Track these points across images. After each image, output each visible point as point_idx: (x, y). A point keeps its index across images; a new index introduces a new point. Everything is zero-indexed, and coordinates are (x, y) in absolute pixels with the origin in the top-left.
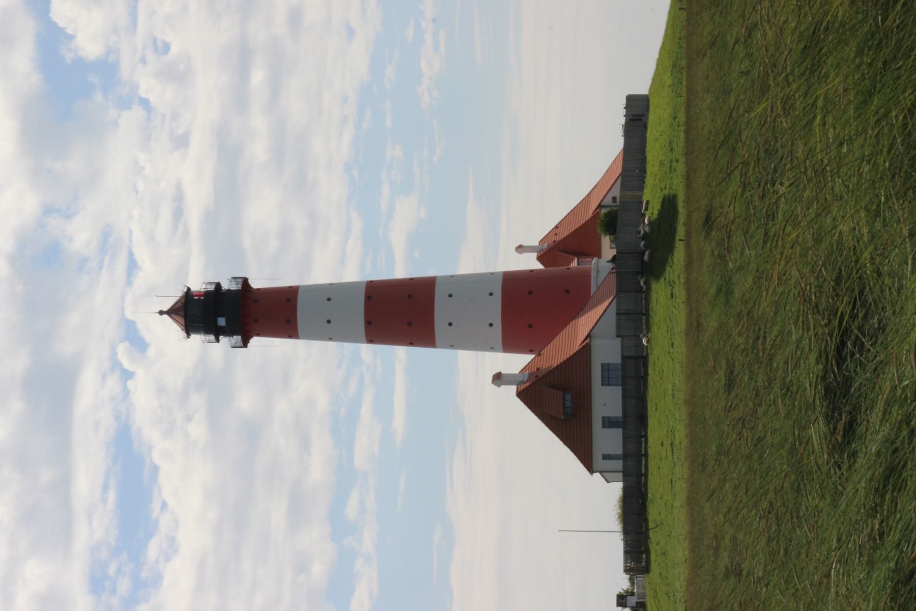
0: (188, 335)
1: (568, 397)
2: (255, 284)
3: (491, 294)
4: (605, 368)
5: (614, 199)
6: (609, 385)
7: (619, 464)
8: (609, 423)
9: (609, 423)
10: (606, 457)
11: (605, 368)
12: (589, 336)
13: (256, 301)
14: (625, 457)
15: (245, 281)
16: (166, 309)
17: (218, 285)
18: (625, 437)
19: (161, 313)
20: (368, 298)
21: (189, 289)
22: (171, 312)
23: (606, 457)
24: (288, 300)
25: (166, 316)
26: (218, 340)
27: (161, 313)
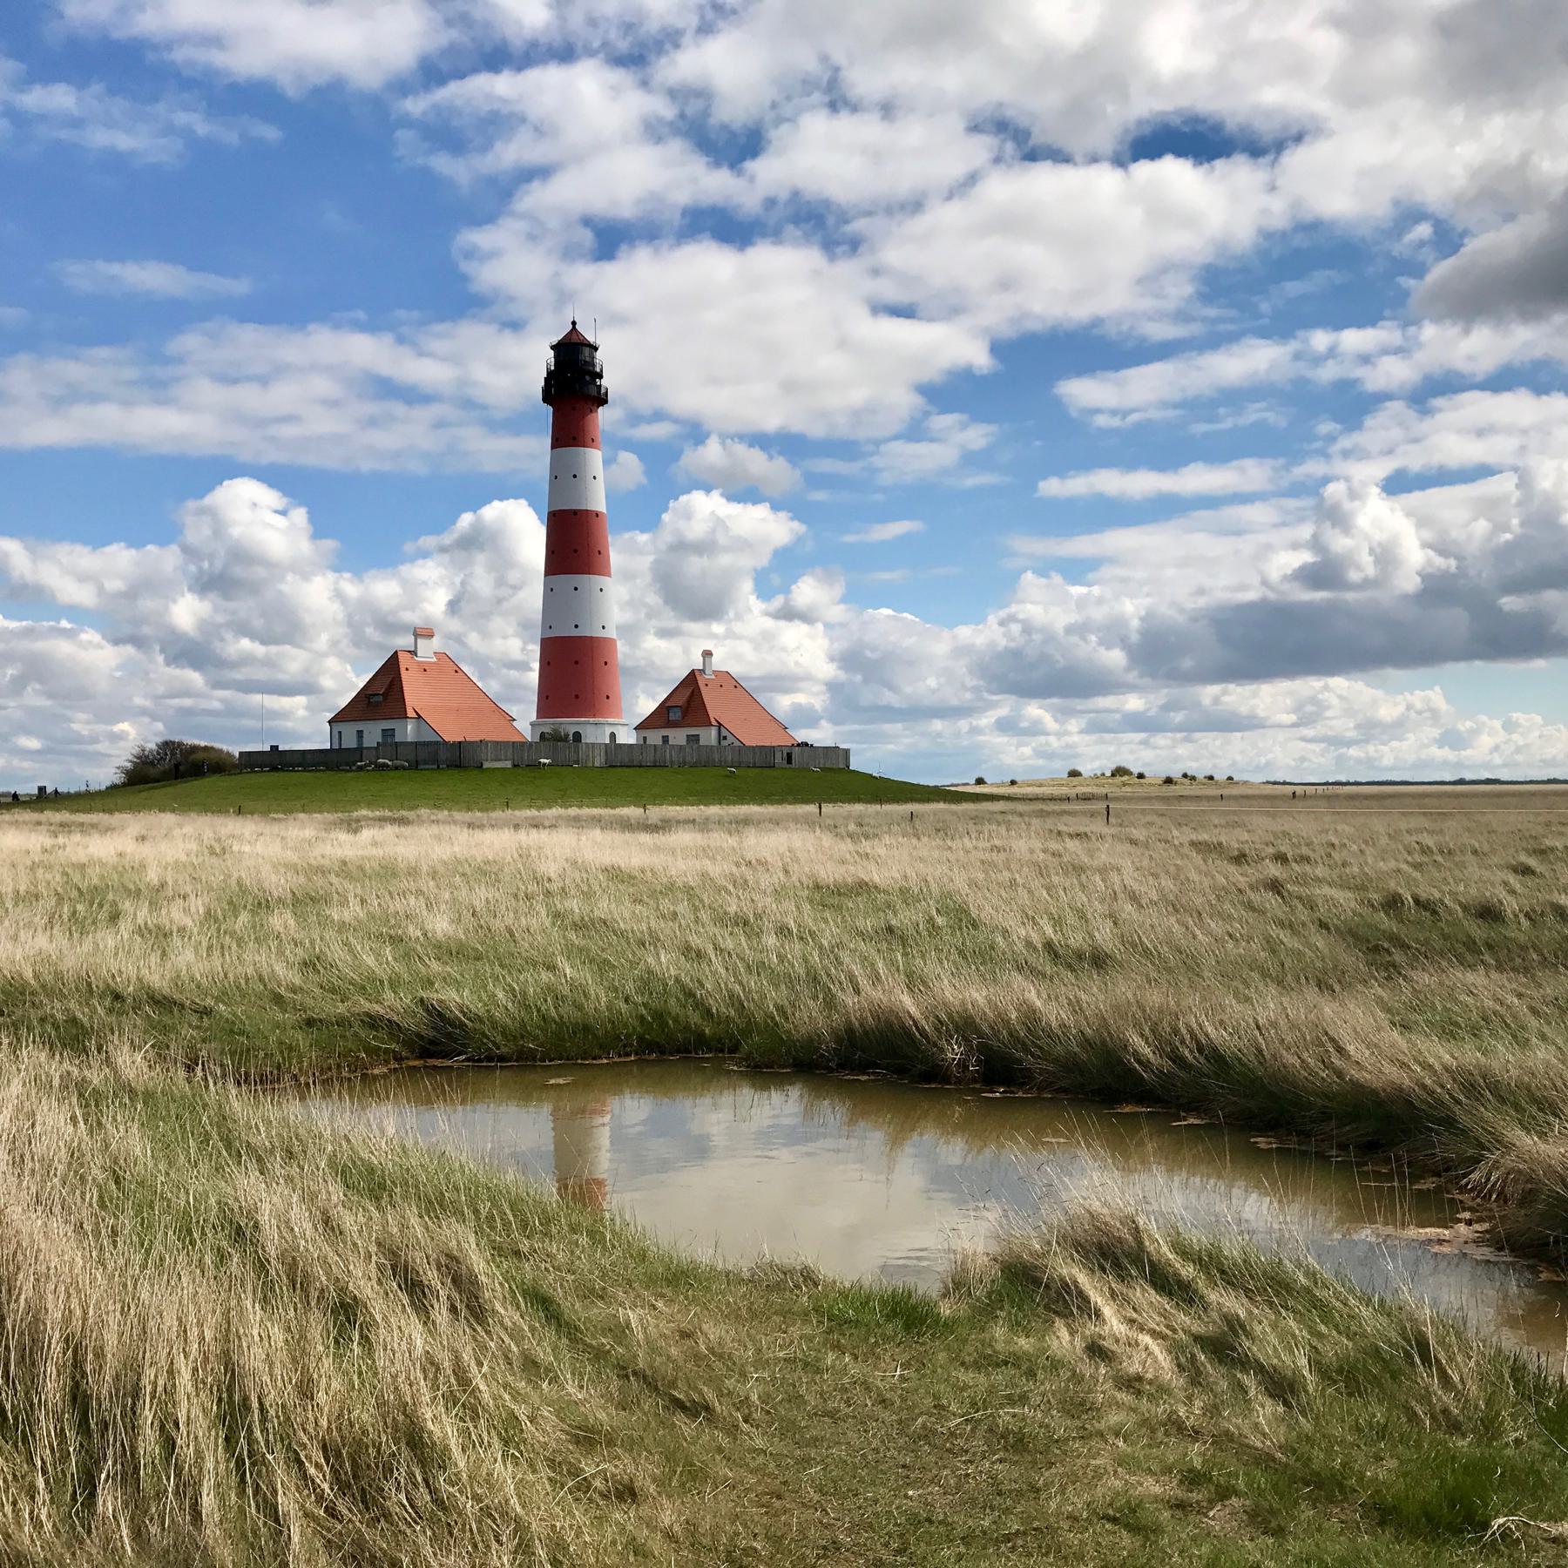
0: (553, 348)
1: (381, 698)
3: (576, 626)
5: (725, 738)
6: (383, 736)
7: (336, 746)
8: (360, 734)
9: (360, 734)
12: (419, 717)
13: (574, 409)
15: (602, 400)
17: (601, 376)
19: (574, 323)
20: (575, 512)
21: (596, 349)
24: (574, 438)
27: (574, 323)
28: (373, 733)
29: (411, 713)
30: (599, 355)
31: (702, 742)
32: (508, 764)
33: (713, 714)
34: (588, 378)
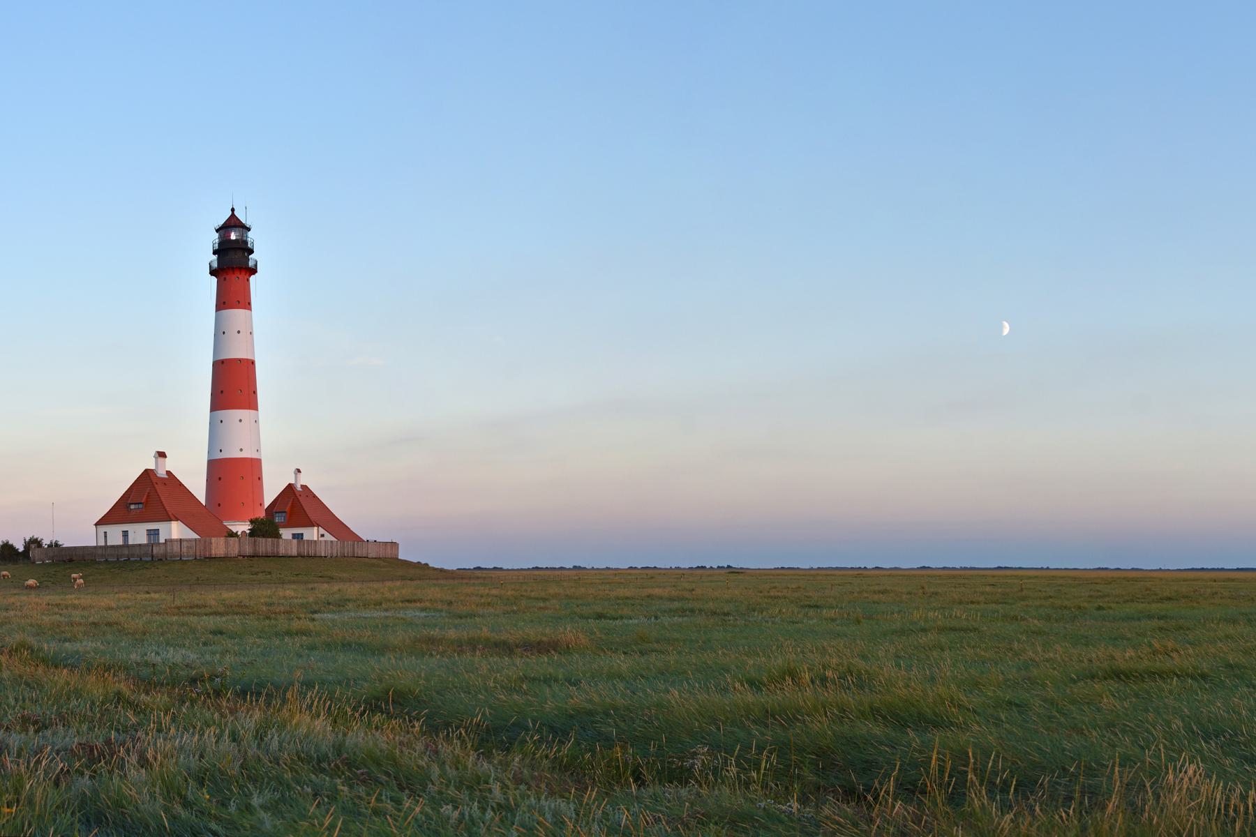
0: (217, 231)
2: (252, 278)
4: (156, 532)
5: (323, 536)
7: (102, 543)
8: (125, 534)
9: (125, 534)
10: (105, 533)
11: (156, 532)
14: (106, 547)
15: (253, 271)
16: (235, 213)
17: (251, 251)
18: (118, 547)
19: (233, 210)
21: (249, 229)
22: (233, 215)
23: (105, 533)
25: (231, 213)
26: (215, 253)
27: (233, 210)
28: (138, 534)
29: (172, 517)
30: (250, 234)
31: (305, 538)
32: (115, 559)
33: (312, 516)
34: (246, 254)
